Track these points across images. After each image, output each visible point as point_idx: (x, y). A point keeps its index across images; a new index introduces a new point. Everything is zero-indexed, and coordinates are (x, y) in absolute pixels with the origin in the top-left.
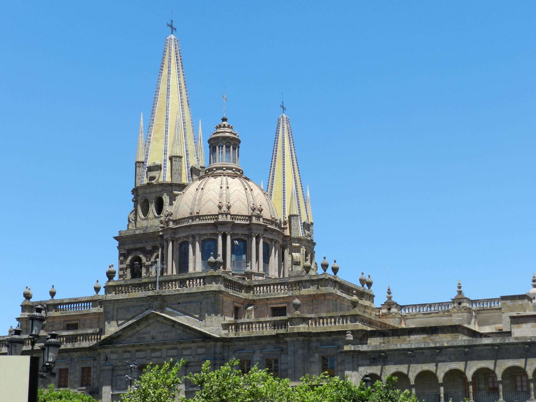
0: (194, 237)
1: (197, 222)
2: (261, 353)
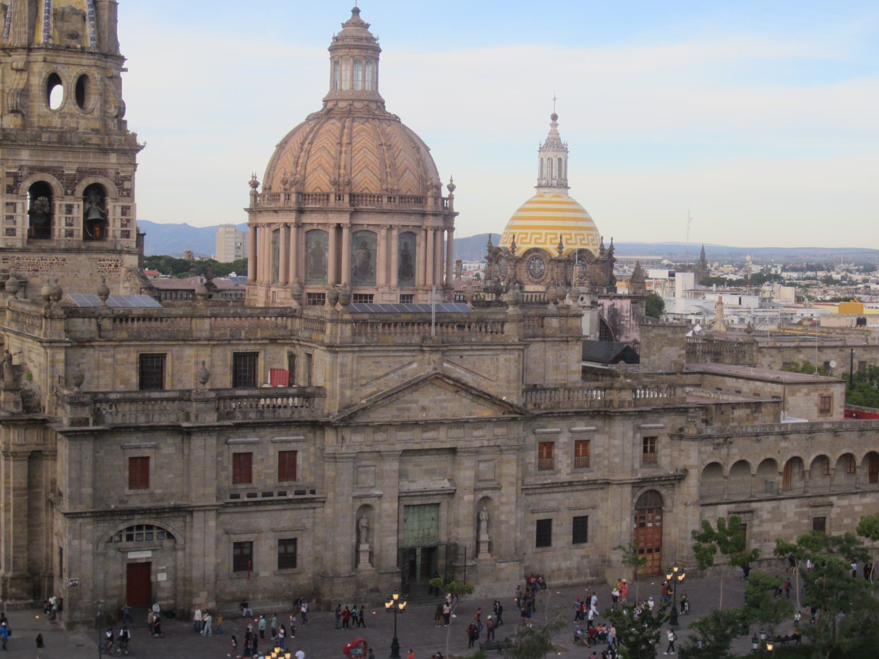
0: (391, 228)
1: (395, 205)
2: (571, 432)
